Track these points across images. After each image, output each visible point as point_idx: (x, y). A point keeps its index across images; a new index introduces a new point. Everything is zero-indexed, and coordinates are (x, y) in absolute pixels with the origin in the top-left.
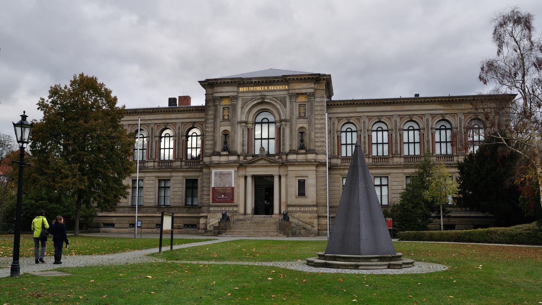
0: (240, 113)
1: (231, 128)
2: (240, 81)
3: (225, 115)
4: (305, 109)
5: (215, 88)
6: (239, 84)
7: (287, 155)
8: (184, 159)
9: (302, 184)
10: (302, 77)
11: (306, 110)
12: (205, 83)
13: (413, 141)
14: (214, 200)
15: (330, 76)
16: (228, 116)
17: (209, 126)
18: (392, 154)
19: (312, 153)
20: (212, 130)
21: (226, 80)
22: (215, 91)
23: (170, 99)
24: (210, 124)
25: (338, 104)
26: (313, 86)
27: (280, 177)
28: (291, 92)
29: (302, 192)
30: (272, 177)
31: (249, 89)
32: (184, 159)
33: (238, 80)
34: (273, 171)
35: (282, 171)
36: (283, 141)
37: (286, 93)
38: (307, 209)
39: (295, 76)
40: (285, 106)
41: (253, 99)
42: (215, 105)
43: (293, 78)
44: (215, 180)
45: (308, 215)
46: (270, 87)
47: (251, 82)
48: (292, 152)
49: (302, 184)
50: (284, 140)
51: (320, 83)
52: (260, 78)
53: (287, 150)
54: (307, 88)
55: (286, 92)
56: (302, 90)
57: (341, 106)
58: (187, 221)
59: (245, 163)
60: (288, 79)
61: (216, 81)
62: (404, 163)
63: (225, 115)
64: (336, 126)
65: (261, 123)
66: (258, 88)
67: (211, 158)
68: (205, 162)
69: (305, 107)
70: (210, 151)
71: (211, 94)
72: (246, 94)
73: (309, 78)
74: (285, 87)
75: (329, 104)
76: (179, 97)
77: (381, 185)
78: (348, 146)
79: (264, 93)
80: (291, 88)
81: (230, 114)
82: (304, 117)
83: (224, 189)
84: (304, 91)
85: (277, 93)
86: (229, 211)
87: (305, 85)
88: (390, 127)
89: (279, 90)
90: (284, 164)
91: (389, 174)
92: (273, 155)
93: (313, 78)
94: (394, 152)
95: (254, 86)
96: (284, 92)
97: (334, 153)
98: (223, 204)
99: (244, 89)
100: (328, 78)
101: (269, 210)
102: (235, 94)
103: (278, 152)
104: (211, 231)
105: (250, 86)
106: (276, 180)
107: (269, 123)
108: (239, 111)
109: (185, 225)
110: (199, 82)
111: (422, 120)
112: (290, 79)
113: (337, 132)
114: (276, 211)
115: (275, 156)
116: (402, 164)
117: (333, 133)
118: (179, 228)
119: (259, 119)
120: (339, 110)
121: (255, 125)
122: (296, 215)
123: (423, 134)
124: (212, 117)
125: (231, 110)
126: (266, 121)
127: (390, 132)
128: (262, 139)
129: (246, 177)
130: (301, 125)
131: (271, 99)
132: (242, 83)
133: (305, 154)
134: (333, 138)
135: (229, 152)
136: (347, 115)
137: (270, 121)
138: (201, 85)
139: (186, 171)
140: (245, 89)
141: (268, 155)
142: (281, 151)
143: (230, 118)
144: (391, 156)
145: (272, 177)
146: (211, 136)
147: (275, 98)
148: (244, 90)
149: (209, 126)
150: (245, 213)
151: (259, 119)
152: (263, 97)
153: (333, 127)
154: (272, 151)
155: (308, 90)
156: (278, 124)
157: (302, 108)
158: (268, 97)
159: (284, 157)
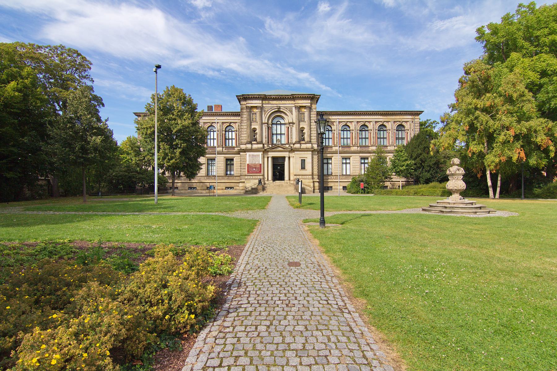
7: (294, 144)
8: (224, 146)
9: (303, 162)
14: (248, 171)
23: (208, 107)
26: (309, 101)
27: (289, 158)
28: (296, 105)
29: (303, 167)
30: (284, 158)
32: (224, 146)
34: (286, 154)
35: (292, 155)
37: (294, 105)
38: (305, 177)
44: (250, 159)
45: (307, 181)
47: (271, 98)
49: (303, 162)
50: (291, 135)
52: (277, 96)
53: (294, 142)
58: (228, 185)
59: (268, 149)
65: (276, 124)
70: (246, 141)
76: (215, 105)
77: (346, 163)
79: (279, 105)
83: (255, 165)
88: (351, 129)
90: (292, 150)
91: (351, 156)
94: (354, 144)
95: (272, 100)
102: (261, 105)
104: (250, 191)
106: (287, 159)
107: (281, 124)
108: (263, 115)
109: (226, 187)
110: (237, 96)
118: (222, 190)
119: (275, 122)
128: (277, 134)
129: (268, 158)
139: (226, 154)
142: (290, 142)
144: (351, 145)
145: (284, 158)
150: (268, 180)
151: (275, 122)
152: (279, 108)
157: (302, 116)
159: (292, 145)
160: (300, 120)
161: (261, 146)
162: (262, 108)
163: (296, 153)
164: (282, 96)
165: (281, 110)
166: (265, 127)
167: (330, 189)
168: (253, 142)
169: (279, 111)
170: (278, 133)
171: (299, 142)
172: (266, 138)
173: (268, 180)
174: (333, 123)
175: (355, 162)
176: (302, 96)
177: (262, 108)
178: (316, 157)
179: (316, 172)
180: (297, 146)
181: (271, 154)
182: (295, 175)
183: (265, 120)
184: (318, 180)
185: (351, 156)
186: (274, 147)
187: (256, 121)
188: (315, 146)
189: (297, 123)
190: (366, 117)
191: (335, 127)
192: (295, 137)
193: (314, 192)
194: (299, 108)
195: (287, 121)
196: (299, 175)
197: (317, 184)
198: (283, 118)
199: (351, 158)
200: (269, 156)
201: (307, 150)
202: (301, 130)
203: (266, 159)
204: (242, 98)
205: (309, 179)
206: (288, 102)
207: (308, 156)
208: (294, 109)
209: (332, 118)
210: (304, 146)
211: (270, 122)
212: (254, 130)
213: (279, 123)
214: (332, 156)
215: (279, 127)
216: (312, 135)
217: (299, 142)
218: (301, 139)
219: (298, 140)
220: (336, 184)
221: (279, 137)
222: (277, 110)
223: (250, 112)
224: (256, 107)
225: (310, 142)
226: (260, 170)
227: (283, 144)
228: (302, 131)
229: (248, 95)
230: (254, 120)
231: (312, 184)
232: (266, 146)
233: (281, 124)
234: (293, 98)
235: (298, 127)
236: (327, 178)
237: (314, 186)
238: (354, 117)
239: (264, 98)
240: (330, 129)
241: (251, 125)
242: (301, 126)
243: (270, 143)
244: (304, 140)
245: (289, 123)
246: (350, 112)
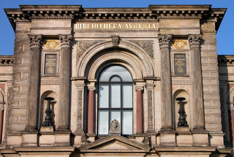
0: (75, 64)
1: (59, 88)
3: (49, 67)
5: (34, 21)
10: (181, 10)
11: (187, 62)
12: (17, 13)
17: (20, 83)
19: (203, 133)
20: (26, 89)
21: (54, 8)
22: (33, 26)
24: (21, 80)
28: (162, 32)
33: (75, 10)
36: (149, 112)
39: (171, 8)
40: (152, 56)
41: (97, 43)
42: (32, 49)
43: (167, 10)
46: (127, 25)
47: (97, 15)
50: (150, 110)
53: (158, 127)
55: (153, 33)
56: (181, 30)
60: (158, 12)
61: (38, 10)
63: (49, 67)
65: (110, 83)
66: (107, 26)
67: (23, 138)
68: (10, 145)
69: (185, 58)
70: (23, 127)
71: (25, 32)
72: (86, 35)
74: (151, 25)
79: (117, 34)
80: (163, 27)
81: (57, 65)
82: (184, 75)
84: (183, 32)
85: (139, 34)
89: (141, 31)
93: (199, 12)
96: (150, 33)
99: (82, 25)
103: (140, 131)
107: (122, 83)
112: (161, 12)
115: (135, 137)
119: (106, 76)
124: (27, 69)
125: (60, 58)
130: (178, 87)
131: (128, 44)
132: (80, 15)
133: (191, 133)
135: (54, 130)
137: (124, 80)
140: (84, 26)
142: (146, 129)
143: (57, 71)
146: (23, 100)
147: (134, 42)
148: (82, 27)
149: (20, 83)
155: (191, 30)
156: (140, 85)
157: (180, 61)
161: (66, 138)
166: (76, 89)
168: (43, 130)
170: (113, 106)
171: (171, 129)
172: (79, 117)
180: (169, 138)
183: (77, 71)
187: (54, 75)
189: (167, 78)
195: (137, 76)
206: (139, 26)
211: (92, 76)
213: (118, 80)
215: (116, 89)
216: (206, 111)
221: (116, 116)
222: (111, 45)
224: (56, 37)
225: (201, 129)
227: (126, 136)
229: (36, 6)
230: (50, 70)
233: (122, 83)
235: (168, 88)
243: (90, 132)
244: (183, 123)
245: (145, 80)
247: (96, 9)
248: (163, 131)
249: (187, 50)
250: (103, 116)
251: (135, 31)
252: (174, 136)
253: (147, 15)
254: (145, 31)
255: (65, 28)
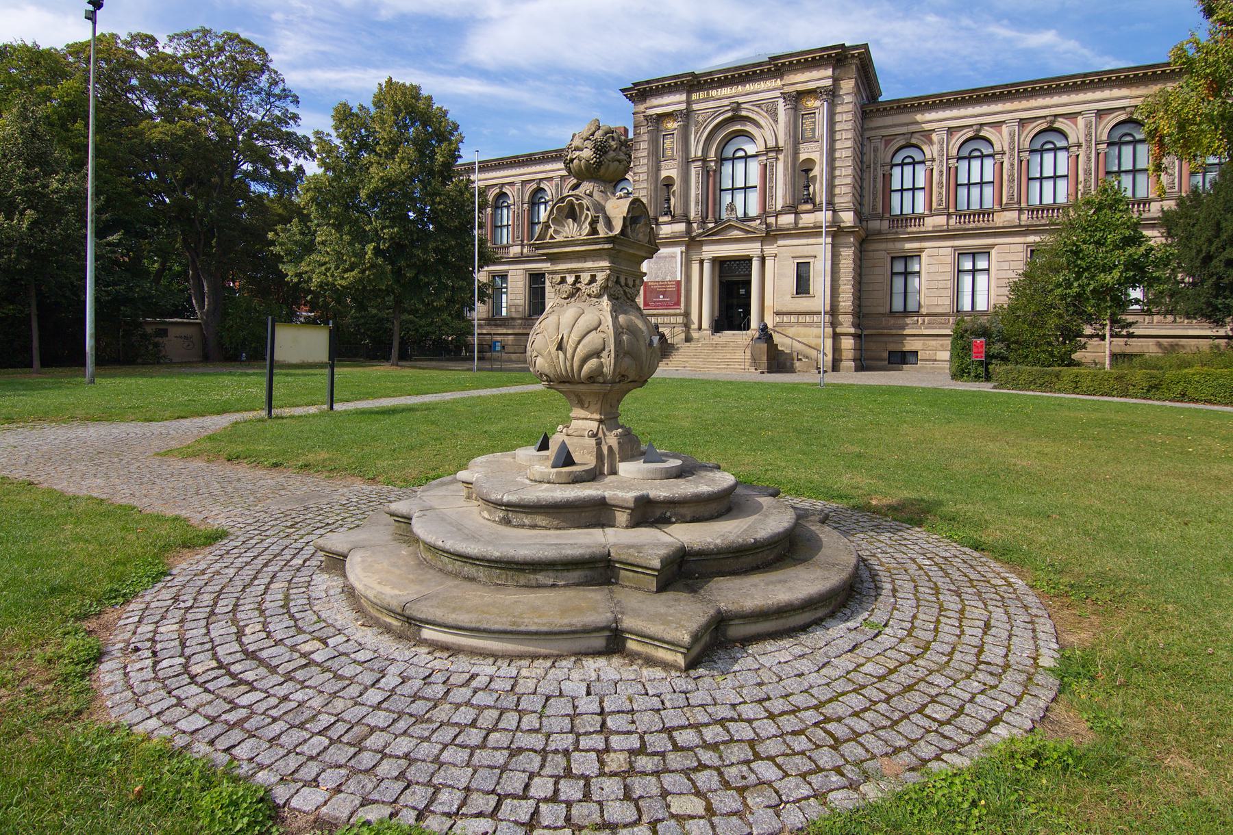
2: (690, 80)
4: (814, 122)
6: (691, 86)
13: (1052, 175)
15: (865, 46)
16: (672, 149)
18: (1001, 205)
25: (885, 109)
28: (786, 90)
30: (748, 260)
31: (708, 94)
34: (751, 249)
35: (769, 250)
37: (777, 93)
40: (776, 121)
47: (712, 80)
48: (784, 211)
51: (844, 66)
53: (779, 208)
54: (820, 77)
57: (892, 112)
59: (700, 235)
62: (1028, 223)
64: (880, 155)
66: (725, 91)
69: (814, 117)
73: (821, 57)
75: (868, 109)
78: (905, 194)
79: (736, 99)
83: (663, 283)
84: (811, 86)
86: (665, 325)
87: (815, 74)
88: (997, 148)
90: (771, 235)
91: (992, 246)
92: (753, 219)
93: (829, 56)
94: (1004, 201)
97: (874, 209)
98: (661, 311)
100: (862, 53)
101: (742, 323)
102: (683, 106)
105: (710, 89)
106: (755, 264)
108: (693, 136)
110: (623, 91)
111: (1076, 125)
112: (783, 64)
113: (882, 166)
114: (754, 323)
116: (1023, 223)
117: (875, 169)
119: (729, 152)
120: (889, 120)
121: (722, 165)
122: (791, 331)
123: (1077, 156)
124: (645, 154)
126: (741, 154)
127: (997, 157)
129: (701, 262)
134: (875, 179)
135: (673, 217)
136: (904, 130)
137: (749, 154)
138: (626, 96)
141: (746, 218)
144: (996, 207)
145: (748, 260)
150: (700, 328)
153: (875, 156)
154: (754, 211)
158: (743, 106)
160: (797, 140)
161: (681, 227)
162: (687, 115)
163: (780, 243)
164: (742, 68)
165: (744, 113)
166: (695, 171)
167: (911, 359)
168: (661, 219)
169: (736, 118)
171: (793, 209)
172: (697, 203)
173: (700, 328)
174: (927, 135)
175: (1005, 265)
176: (802, 58)
177: (687, 115)
178: (847, 256)
179: (846, 301)
180: (787, 220)
181: (711, 251)
182: (778, 313)
183: (696, 150)
184: (852, 330)
185: (992, 246)
186: (718, 229)
188: (848, 218)
190: (1056, 100)
191: (935, 148)
192: (780, 198)
193: (835, 368)
194: (797, 98)
196: (806, 314)
197: (848, 344)
198: (751, 138)
199: (993, 252)
200: (704, 256)
201: (814, 231)
202: (803, 171)
203: (695, 267)
204: (640, 92)
205: (817, 325)
206: (763, 85)
207: (819, 251)
208: (781, 100)
209: (928, 118)
210: (807, 220)
211: (712, 154)
212: (668, 183)
214: (922, 250)
217: (793, 209)
218: (801, 198)
219: (789, 202)
220: (933, 343)
222: (729, 114)
223: (658, 130)
226: (675, 299)
228: (807, 171)
229: (648, 82)
230: (669, 153)
231: (829, 342)
232: (695, 225)
233: (746, 157)
234: (777, 67)
235: (789, 159)
236: (900, 322)
237: (836, 349)
238: (1008, 106)
239: (693, 83)
240: (918, 157)
241: (658, 170)
242: (803, 157)
243: (710, 218)
246: (992, 88)
247: (710, 73)
248: (784, 211)
249: (817, 108)
250: (727, 198)
251: (757, 93)
252: (793, 216)
253: (769, 70)
254: (768, 90)
255: (680, 103)
